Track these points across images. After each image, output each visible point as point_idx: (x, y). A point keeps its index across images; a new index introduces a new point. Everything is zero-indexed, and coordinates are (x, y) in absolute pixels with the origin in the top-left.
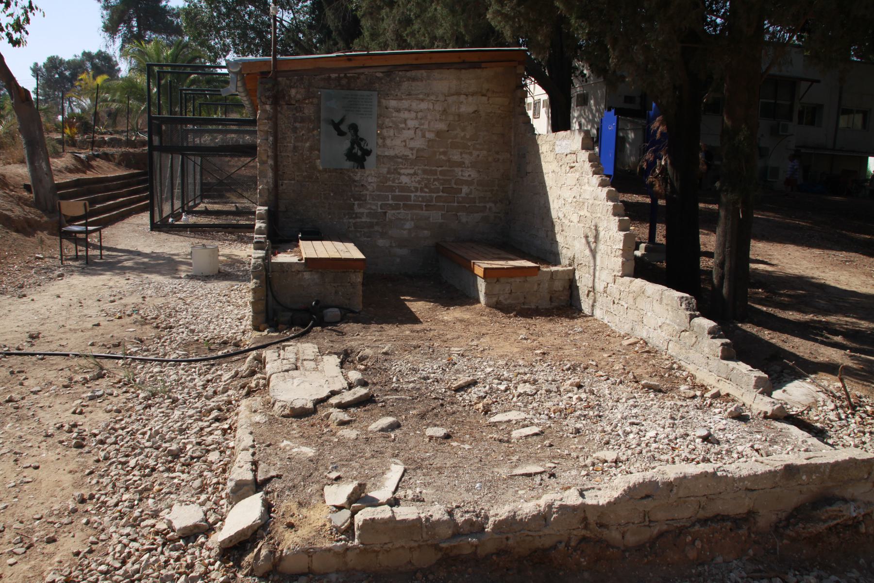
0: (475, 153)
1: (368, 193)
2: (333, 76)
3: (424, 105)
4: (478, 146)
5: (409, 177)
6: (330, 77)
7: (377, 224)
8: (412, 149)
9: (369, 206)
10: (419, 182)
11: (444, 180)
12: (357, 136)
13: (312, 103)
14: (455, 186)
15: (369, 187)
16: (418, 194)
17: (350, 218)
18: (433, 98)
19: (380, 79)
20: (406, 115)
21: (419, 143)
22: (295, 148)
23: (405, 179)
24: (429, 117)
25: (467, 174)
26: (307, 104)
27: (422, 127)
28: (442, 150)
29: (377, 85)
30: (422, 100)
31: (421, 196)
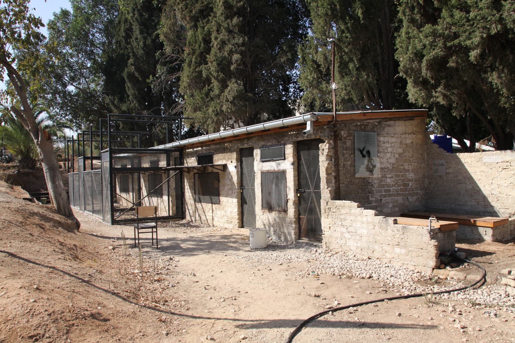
0: (413, 164)
1: (374, 189)
2: (359, 124)
3: (393, 140)
4: (414, 161)
6: (357, 124)
7: (379, 206)
8: (390, 163)
9: (375, 196)
10: (394, 181)
11: (403, 179)
13: (350, 139)
14: (407, 183)
15: (375, 186)
16: (394, 188)
17: (368, 204)
18: (396, 136)
20: (387, 145)
21: (392, 160)
22: (344, 165)
23: (388, 180)
24: (396, 146)
25: (410, 176)
26: (348, 140)
28: (401, 163)
30: (393, 137)
31: (395, 189)
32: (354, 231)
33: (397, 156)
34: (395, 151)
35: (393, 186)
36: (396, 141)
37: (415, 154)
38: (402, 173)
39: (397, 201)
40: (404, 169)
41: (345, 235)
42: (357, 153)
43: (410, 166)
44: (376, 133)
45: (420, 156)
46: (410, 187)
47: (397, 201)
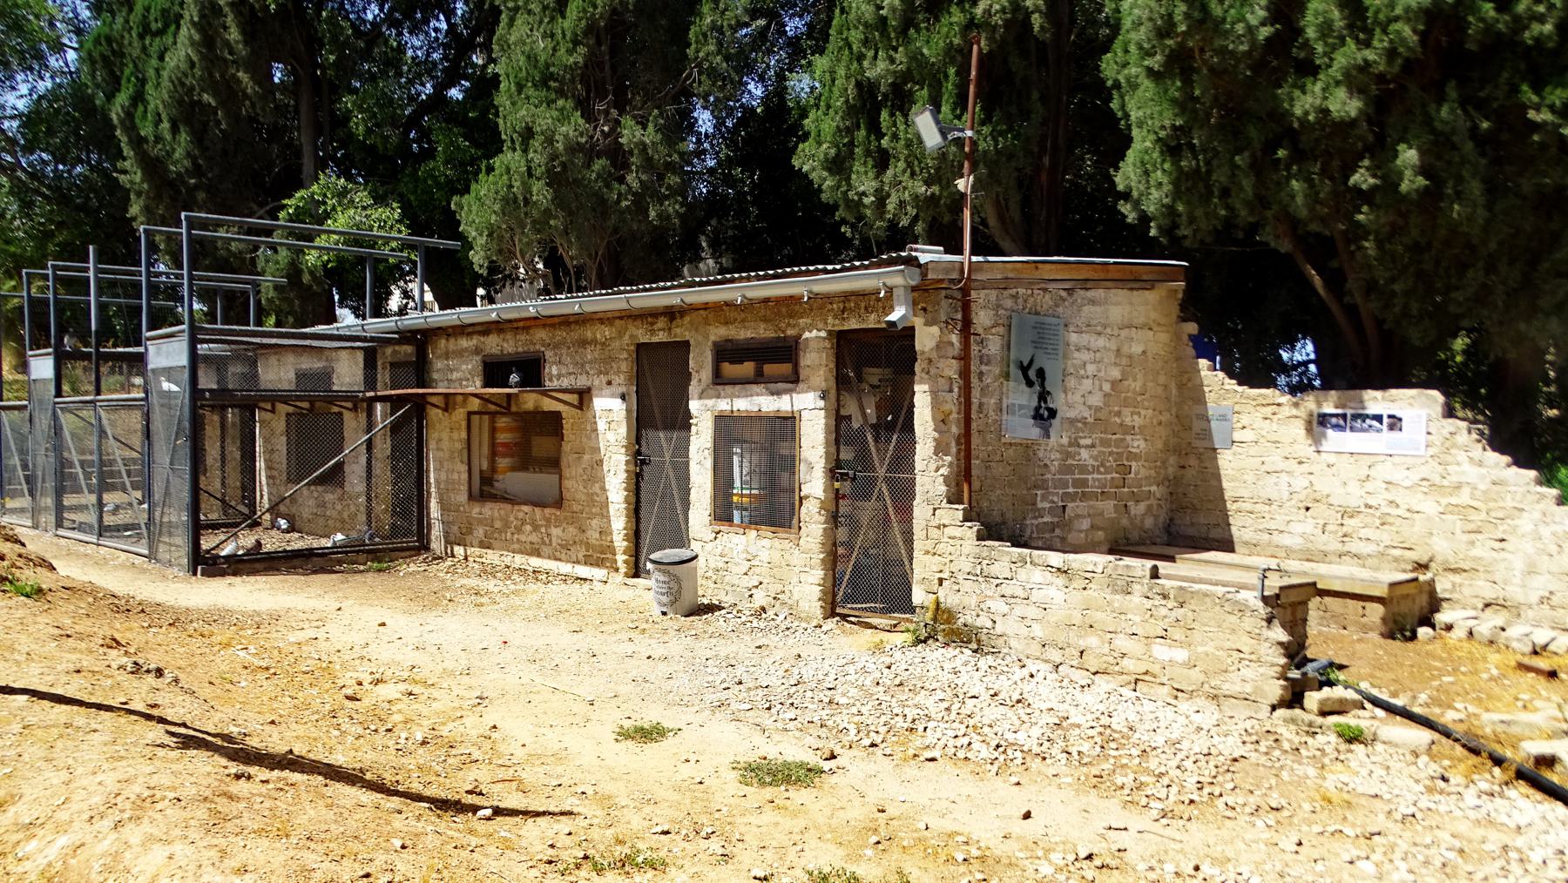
0: (1143, 412)
3: (1101, 342)
4: (1146, 403)
8: (1090, 407)
16: (1095, 476)
17: (1036, 518)
18: (1109, 331)
19: (1064, 300)
20: (1085, 356)
22: (981, 405)
25: (1136, 444)
28: (1116, 409)
30: (1099, 334)
32: (1020, 593)
33: (1107, 387)
35: (1096, 470)
37: (1150, 384)
39: (1102, 514)
41: (989, 603)
42: (1015, 371)
43: (1136, 417)
45: (1160, 390)
46: (1132, 475)
47: (1102, 514)
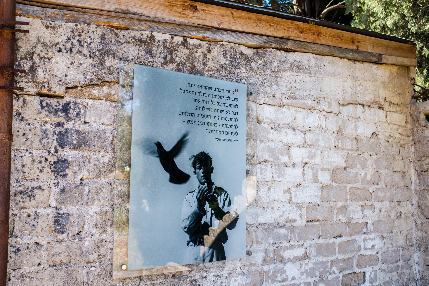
0: (377, 205)
2: (160, 37)
4: (380, 194)
5: (298, 263)
6: (152, 38)
8: (299, 206)
10: (310, 273)
11: (344, 260)
12: (210, 184)
14: (357, 270)
18: (324, 106)
19: (249, 60)
24: (322, 143)
25: (370, 246)
26: (94, 98)
27: (313, 160)
28: (340, 204)
29: (242, 72)
30: (311, 109)
34: (317, 161)
36: (324, 125)
37: (383, 172)
38: (344, 239)
40: (348, 223)
43: (368, 212)
44: (243, 88)
45: (397, 178)
